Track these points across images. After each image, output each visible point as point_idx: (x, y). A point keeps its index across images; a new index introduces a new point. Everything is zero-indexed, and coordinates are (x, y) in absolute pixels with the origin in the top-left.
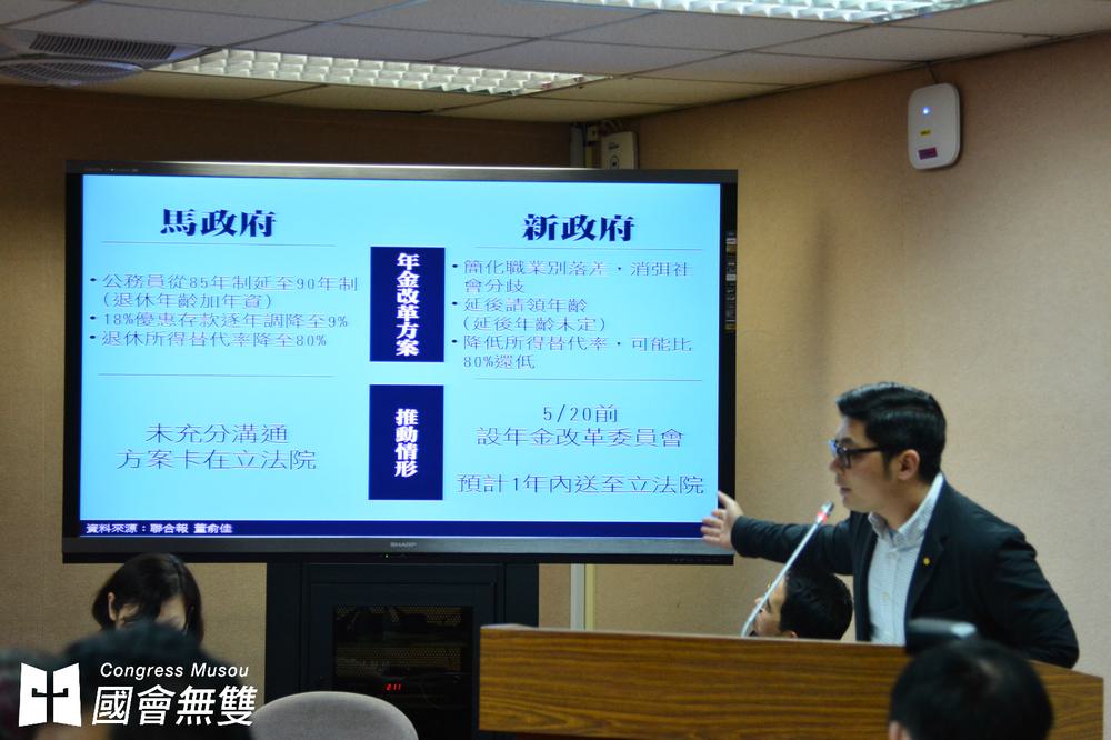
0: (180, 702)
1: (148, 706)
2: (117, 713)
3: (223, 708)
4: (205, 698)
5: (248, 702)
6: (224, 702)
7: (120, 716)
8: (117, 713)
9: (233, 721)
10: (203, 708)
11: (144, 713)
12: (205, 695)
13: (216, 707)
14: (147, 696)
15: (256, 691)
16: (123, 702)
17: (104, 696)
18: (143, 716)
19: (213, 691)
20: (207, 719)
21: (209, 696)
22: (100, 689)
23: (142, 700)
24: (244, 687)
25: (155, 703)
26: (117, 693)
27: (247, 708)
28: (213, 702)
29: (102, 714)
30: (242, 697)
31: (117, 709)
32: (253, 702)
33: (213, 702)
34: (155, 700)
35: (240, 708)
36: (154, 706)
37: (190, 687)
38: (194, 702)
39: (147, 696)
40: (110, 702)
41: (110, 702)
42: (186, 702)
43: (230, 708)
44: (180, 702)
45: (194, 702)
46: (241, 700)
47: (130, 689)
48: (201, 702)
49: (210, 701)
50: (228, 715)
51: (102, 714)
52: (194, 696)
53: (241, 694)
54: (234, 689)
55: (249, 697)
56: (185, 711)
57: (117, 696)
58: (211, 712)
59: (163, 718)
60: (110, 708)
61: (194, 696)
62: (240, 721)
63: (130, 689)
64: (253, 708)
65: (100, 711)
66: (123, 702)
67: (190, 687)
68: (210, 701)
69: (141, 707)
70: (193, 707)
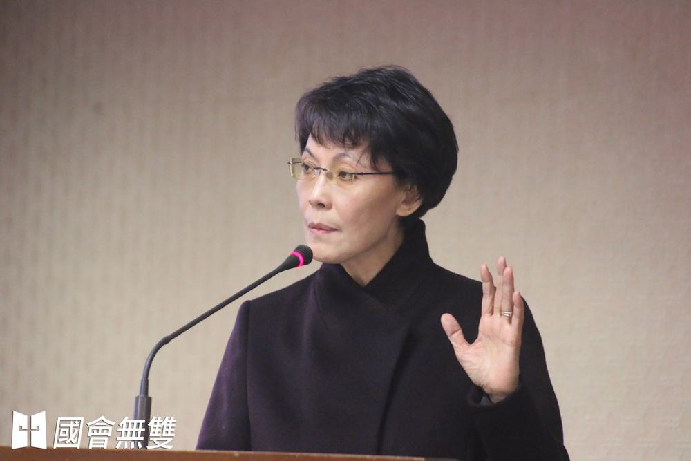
0: (119, 430)
1: (96, 434)
2: (72, 439)
3: (151, 434)
4: (138, 427)
5: (170, 430)
6: (152, 430)
7: (74, 441)
8: (72, 439)
9: (159, 445)
10: (136, 435)
11: (92, 439)
12: (138, 427)
13: (146, 434)
14: (95, 425)
15: (175, 421)
16: (77, 430)
17: (62, 426)
18: (91, 442)
19: (144, 421)
20: (139, 444)
21: (141, 425)
22: (60, 419)
23: (91, 428)
24: (167, 418)
25: (100, 431)
26: (72, 422)
27: (169, 434)
28: (144, 430)
29: (60, 440)
30: (166, 425)
31: (72, 436)
32: (174, 425)
33: (144, 430)
34: (100, 428)
35: (164, 434)
36: (100, 434)
37: (127, 418)
38: (129, 430)
39: (95, 425)
40: (67, 430)
41: (67, 430)
42: (123, 430)
43: (157, 435)
44: (119, 430)
45: (129, 430)
46: (165, 428)
47: (82, 419)
48: (135, 430)
49: (142, 430)
50: (155, 439)
51: (60, 440)
52: (130, 425)
53: (165, 424)
54: (159, 420)
55: (170, 426)
56: (123, 438)
57: (72, 425)
58: (142, 438)
59: (106, 443)
60: (67, 435)
61: (130, 425)
62: (163, 445)
63: (82, 419)
64: (173, 435)
65: (59, 437)
66: (77, 430)
67: (127, 418)
68: (142, 430)
69: (90, 434)
70: (129, 434)
